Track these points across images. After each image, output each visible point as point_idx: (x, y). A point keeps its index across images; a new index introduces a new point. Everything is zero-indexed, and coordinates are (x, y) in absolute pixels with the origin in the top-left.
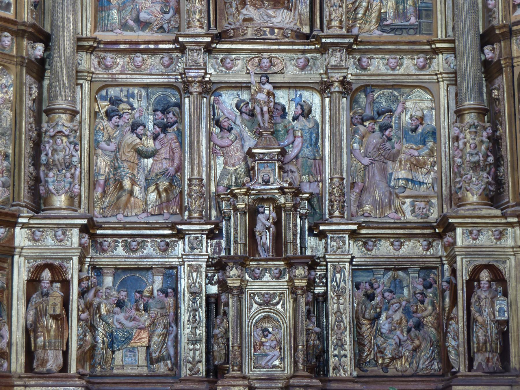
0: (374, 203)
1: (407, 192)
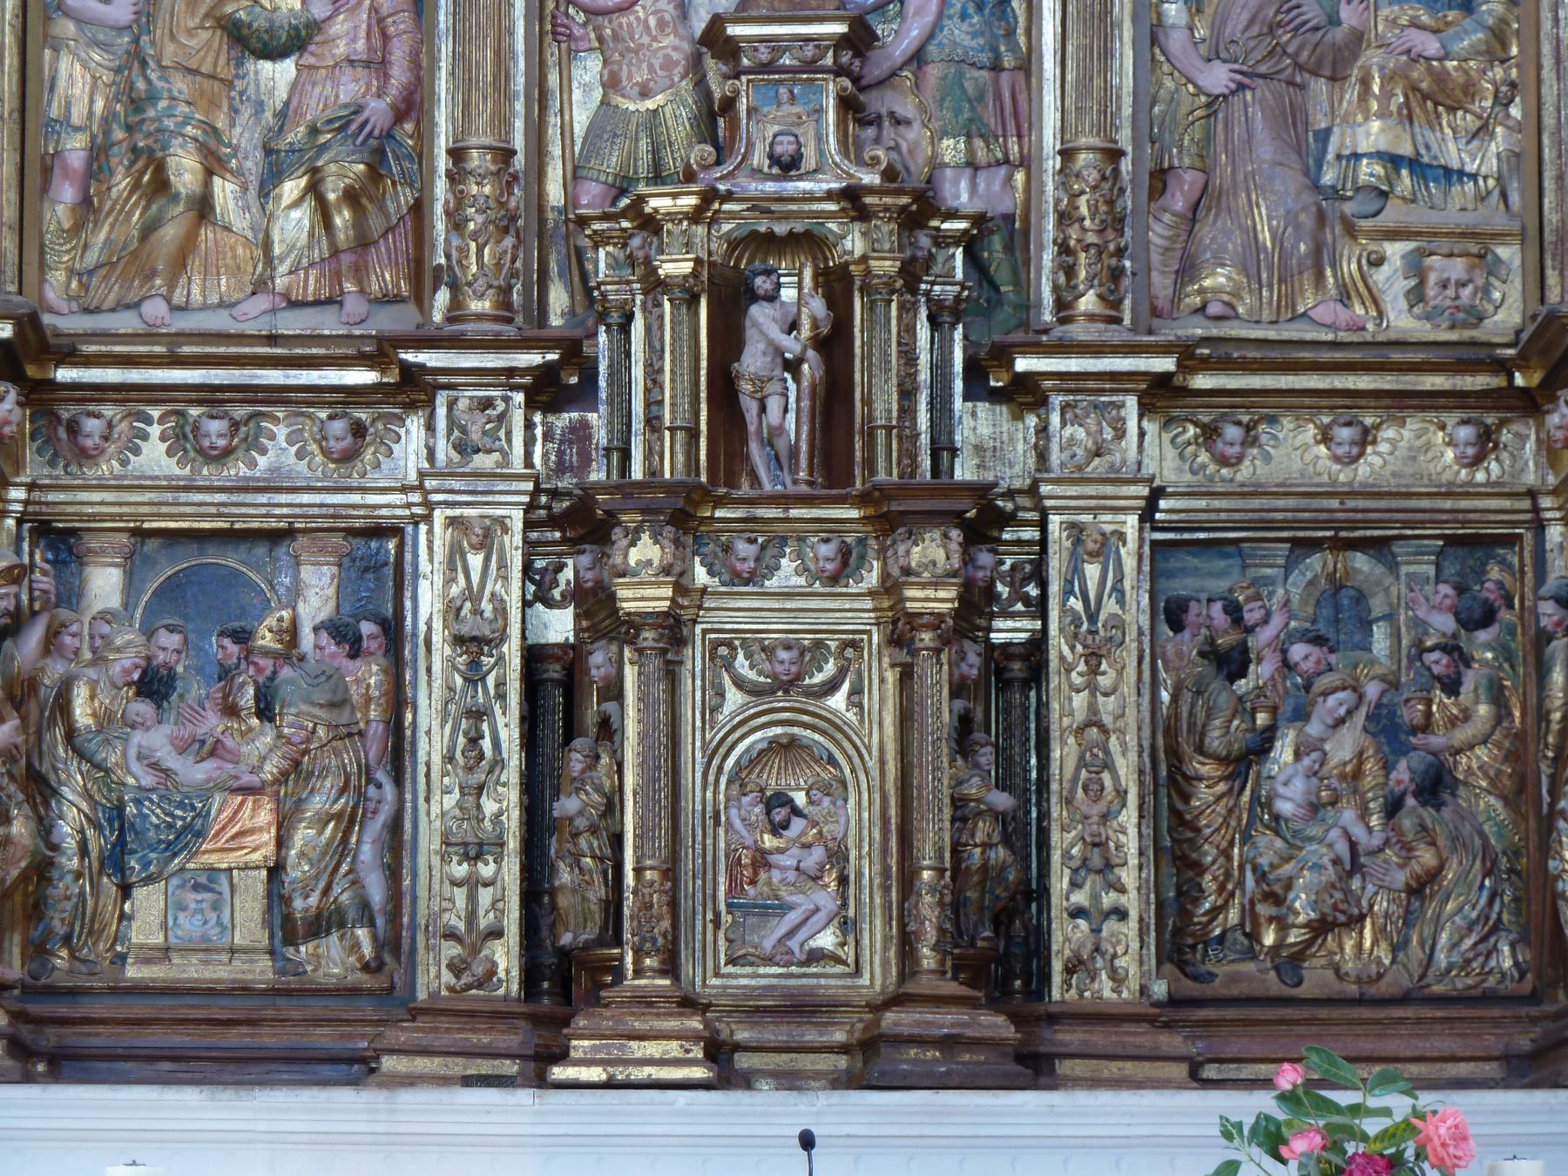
0: (1250, 261)
1: (1393, 215)
